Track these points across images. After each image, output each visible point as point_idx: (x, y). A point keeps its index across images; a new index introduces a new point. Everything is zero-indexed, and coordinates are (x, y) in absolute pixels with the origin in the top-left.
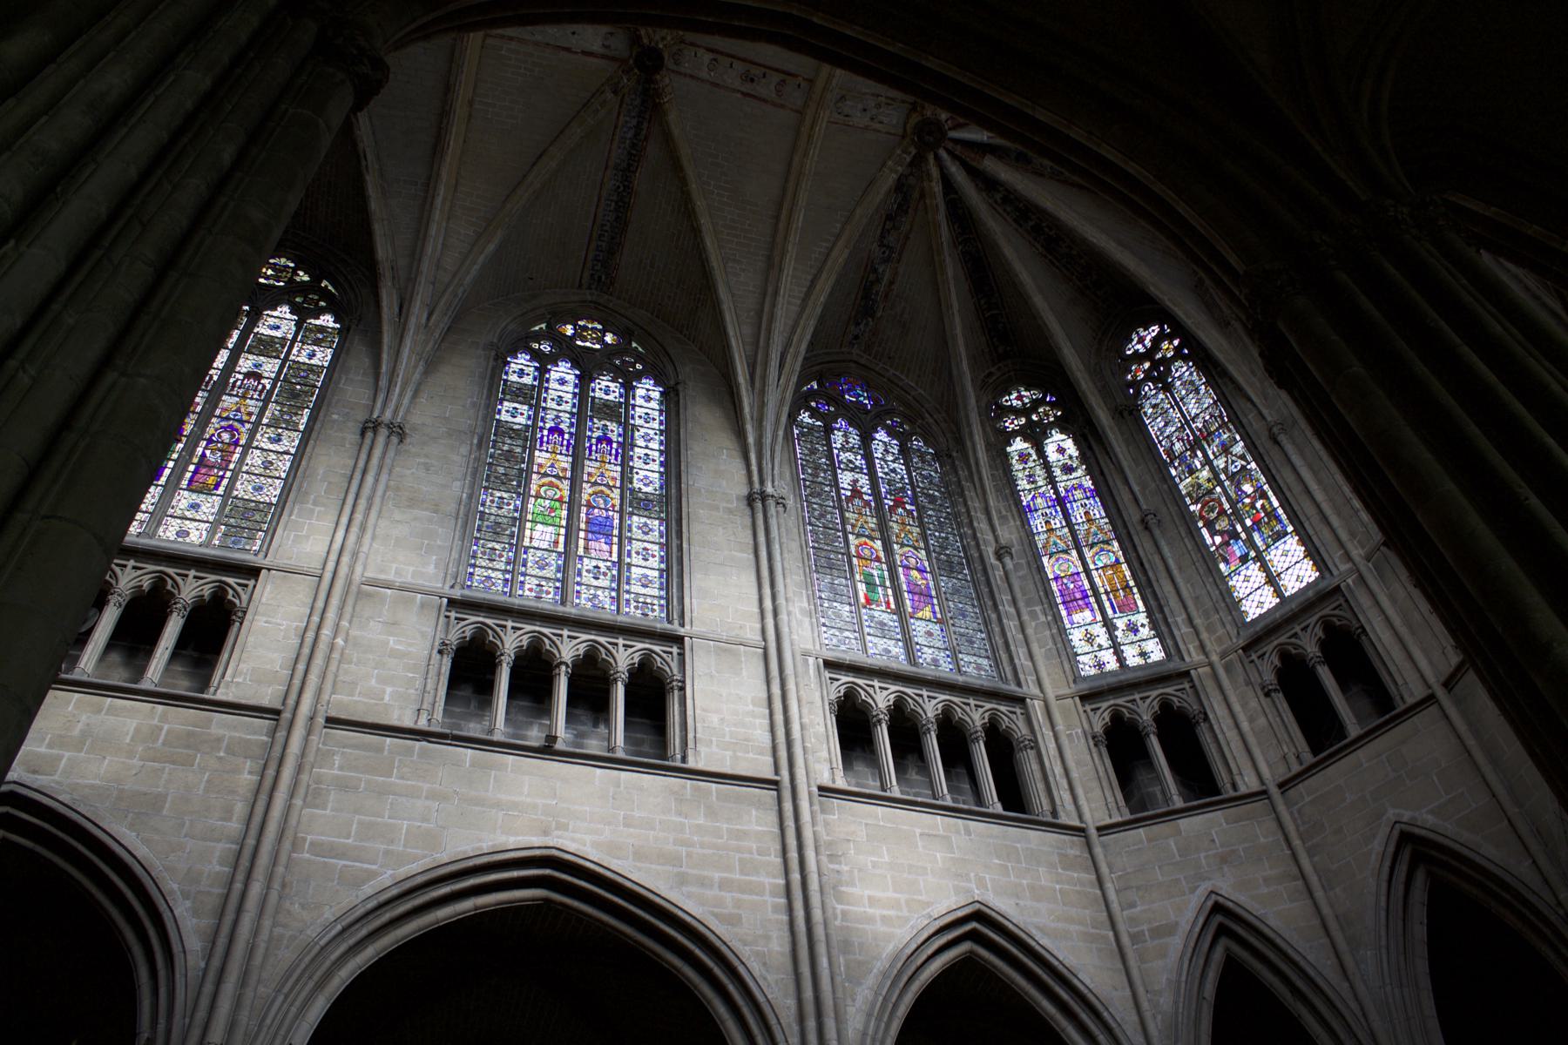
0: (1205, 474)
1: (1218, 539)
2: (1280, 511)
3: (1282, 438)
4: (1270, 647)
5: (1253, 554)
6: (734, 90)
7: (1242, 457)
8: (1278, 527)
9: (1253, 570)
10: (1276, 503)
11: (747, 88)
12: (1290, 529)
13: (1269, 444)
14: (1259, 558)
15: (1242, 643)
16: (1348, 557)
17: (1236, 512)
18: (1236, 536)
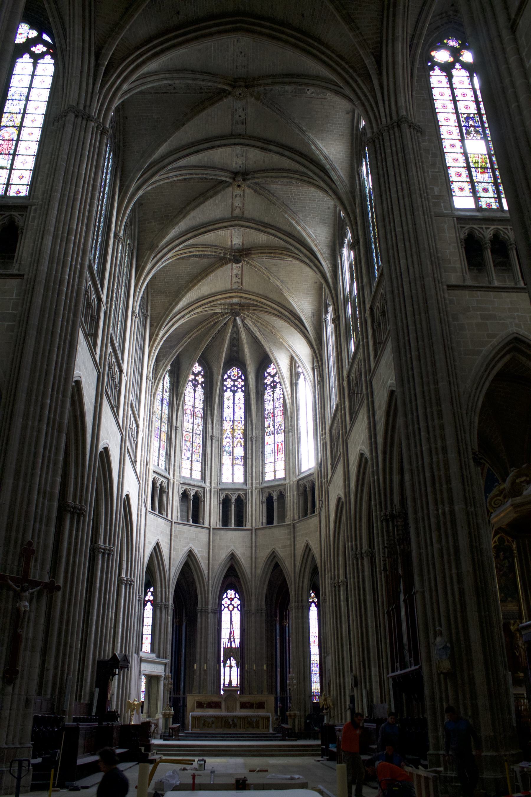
0: (191, 426)
1: (186, 448)
2: (201, 455)
3: (214, 441)
4: (185, 487)
5: (190, 459)
6: (232, 273)
7: (200, 431)
8: (198, 458)
9: (189, 462)
10: (201, 452)
11: (233, 276)
12: (201, 461)
13: (210, 438)
14: (191, 461)
15: (181, 482)
16: (211, 483)
17: (192, 444)
18: (189, 451)
